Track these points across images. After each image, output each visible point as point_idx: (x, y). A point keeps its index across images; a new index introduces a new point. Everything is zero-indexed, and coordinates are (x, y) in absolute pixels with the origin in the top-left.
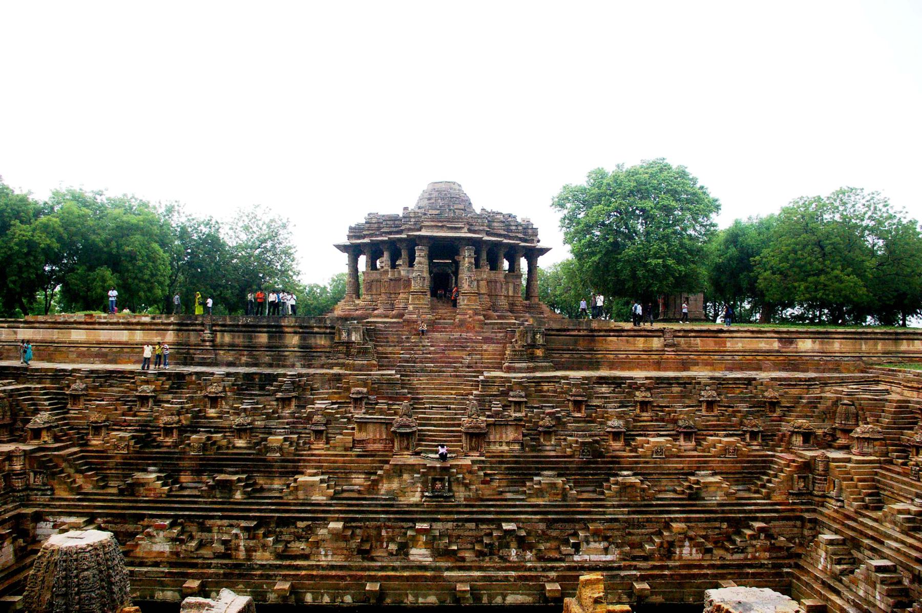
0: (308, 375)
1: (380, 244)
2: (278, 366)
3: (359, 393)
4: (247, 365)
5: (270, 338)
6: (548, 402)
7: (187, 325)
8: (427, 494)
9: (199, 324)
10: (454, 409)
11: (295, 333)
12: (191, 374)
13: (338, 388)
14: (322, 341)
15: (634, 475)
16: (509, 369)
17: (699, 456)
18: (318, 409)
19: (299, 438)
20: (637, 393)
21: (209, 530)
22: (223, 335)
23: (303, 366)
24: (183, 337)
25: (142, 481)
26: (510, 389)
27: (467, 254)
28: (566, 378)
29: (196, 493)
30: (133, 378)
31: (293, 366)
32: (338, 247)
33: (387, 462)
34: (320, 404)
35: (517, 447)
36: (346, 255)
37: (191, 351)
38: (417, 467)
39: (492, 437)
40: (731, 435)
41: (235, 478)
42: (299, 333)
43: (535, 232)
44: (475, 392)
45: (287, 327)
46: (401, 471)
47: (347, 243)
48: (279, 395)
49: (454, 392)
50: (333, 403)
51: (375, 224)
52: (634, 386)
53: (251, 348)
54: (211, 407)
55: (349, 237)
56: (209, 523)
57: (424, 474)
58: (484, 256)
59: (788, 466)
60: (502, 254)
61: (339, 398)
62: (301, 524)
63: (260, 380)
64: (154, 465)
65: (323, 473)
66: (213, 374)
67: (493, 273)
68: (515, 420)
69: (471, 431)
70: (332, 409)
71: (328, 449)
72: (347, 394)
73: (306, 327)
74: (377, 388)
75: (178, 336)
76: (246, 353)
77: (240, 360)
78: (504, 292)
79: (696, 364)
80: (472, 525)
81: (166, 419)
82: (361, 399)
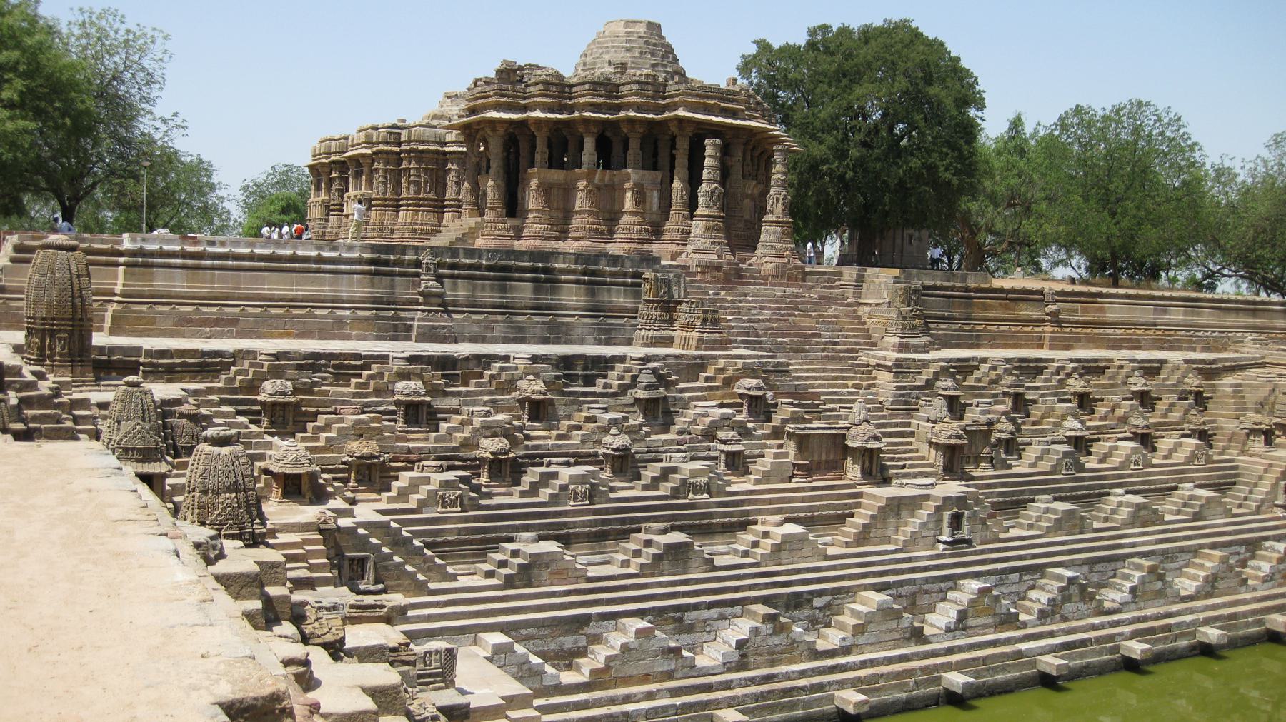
2: (557, 341)
4: (506, 340)
5: (536, 291)
6: (982, 396)
7: (387, 263)
9: (410, 264)
11: (577, 282)
12: (467, 359)
13: (707, 379)
20: (1071, 381)
21: (690, 629)
22: (454, 288)
23: (599, 342)
31: (582, 342)
37: (403, 314)
42: (584, 283)
45: (562, 271)
46: (899, 506)
56: (690, 616)
62: (818, 602)
64: (526, 528)
69: (953, 442)
72: (727, 390)
73: (593, 273)
76: (499, 318)
79: (1079, 340)
80: (1014, 577)
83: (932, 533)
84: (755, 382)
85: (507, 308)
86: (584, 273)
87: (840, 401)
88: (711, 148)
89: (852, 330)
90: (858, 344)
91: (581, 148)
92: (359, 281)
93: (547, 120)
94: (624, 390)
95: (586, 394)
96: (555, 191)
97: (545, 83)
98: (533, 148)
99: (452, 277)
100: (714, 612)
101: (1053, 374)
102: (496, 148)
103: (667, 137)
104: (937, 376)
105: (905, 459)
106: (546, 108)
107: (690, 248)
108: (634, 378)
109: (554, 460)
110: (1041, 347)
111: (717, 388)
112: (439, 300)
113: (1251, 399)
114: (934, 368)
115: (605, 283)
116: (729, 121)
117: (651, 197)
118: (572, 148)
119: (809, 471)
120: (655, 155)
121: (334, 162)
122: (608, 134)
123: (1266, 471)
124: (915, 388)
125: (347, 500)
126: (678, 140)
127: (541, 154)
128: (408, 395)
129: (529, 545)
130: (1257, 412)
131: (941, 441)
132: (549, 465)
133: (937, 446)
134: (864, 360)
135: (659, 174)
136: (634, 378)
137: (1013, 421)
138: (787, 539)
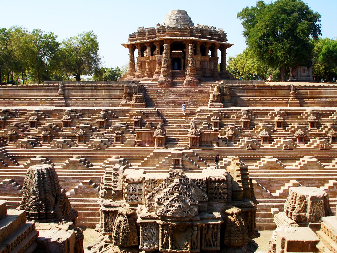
0: (111, 110)
1: (144, 43)
3: (138, 118)
4: (82, 106)
7: (51, 86)
10: (184, 126)
11: (105, 89)
15: (274, 157)
16: (211, 106)
17: (306, 149)
18: (118, 127)
19: (109, 141)
20: (276, 118)
26: (212, 115)
27: (190, 48)
28: (240, 110)
29: (60, 167)
30: (26, 113)
32: (123, 45)
33: (152, 152)
34: (118, 124)
36: (128, 49)
37: (54, 99)
39: (203, 139)
40: (322, 139)
41: (79, 160)
43: (225, 35)
44: (194, 118)
47: (129, 43)
48: (98, 120)
49: (184, 118)
50: (124, 124)
51: (142, 33)
52: (274, 115)
54: (65, 126)
55: (130, 40)
57: (169, 157)
58: (199, 48)
60: (208, 46)
61: (128, 121)
65: (121, 157)
66: (65, 110)
67: (203, 58)
68: (215, 131)
70: (124, 126)
71: (122, 146)
73: (110, 86)
74: (145, 116)
78: (209, 67)
81: (44, 132)
82: (138, 121)
86: (107, 86)
92: (43, 91)
94: (95, 119)
100: (75, 180)
104: (212, 115)
106: (140, 40)
109: (61, 137)
110: (287, 106)
115: (113, 89)
116: (184, 38)
119: (142, 144)
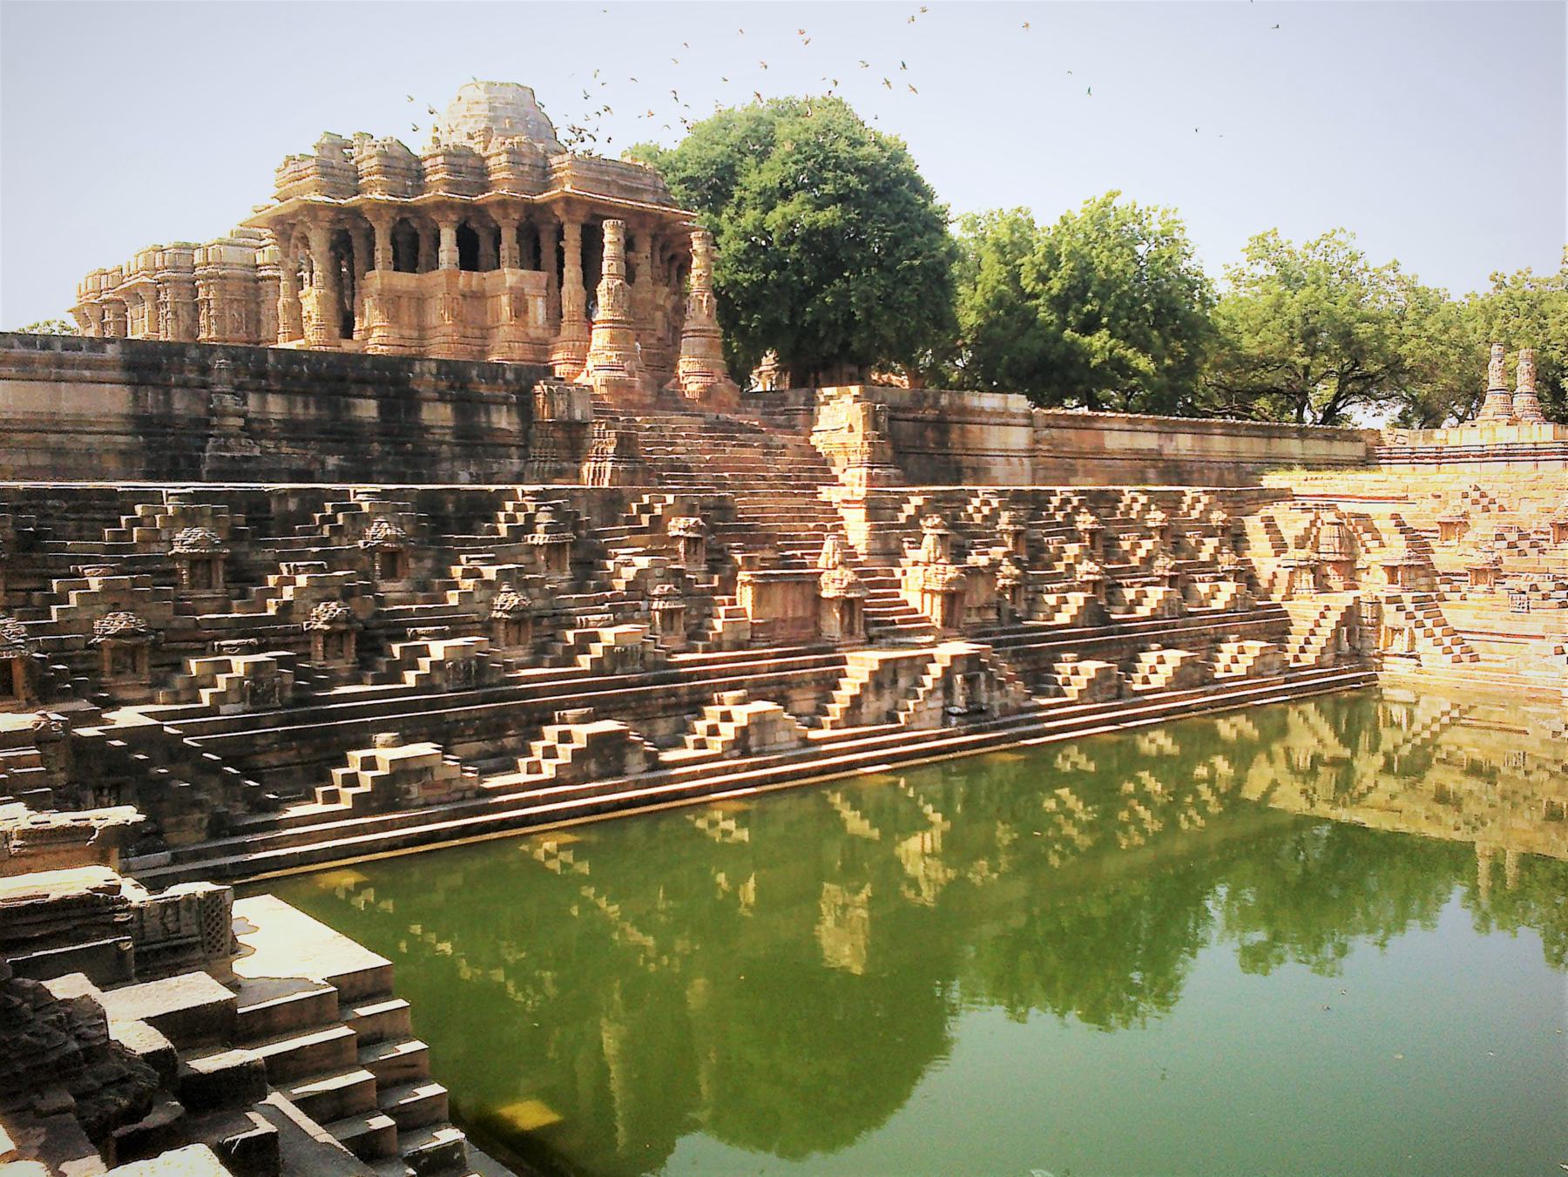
5: (381, 408)
8: (956, 710)
11: (442, 399)
12: (283, 496)
14: (503, 420)
22: (264, 402)
24: (150, 398)
25: (417, 766)
31: (453, 479)
35: (992, 615)
38: (918, 662)
46: (895, 673)
49: (811, 525)
53: (344, 435)
59: (1323, 616)
63: (458, 508)
75: (136, 399)
77: (323, 464)
83: (940, 703)
84: (692, 520)
85: (344, 435)
87: (801, 547)
88: (610, 235)
89: (805, 462)
90: (816, 479)
91: (438, 243)
92: (112, 393)
93: (389, 205)
94: (517, 533)
95: (464, 542)
96: (404, 301)
97: (384, 155)
98: (371, 245)
99: (257, 390)
101: (1058, 509)
102: (319, 241)
103: (551, 227)
104: (920, 512)
105: (894, 613)
107: (590, 365)
108: (530, 518)
109: (420, 630)
111: (642, 531)
112: (241, 422)
113: (1289, 534)
114: (917, 501)
117: (535, 307)
118: (424, 247)
120: (537, 251)
121: (106, 302)
122: (473, 225)
123: (1323, 616)
124: (901, 526)
125: (95, 701)
126: (566, 227)
127: (383, 249)
128: (192, 546)
129: (386, 753)
130: (1300, 545)
131: (939, 588)
132: (416, 636)
133: (932, 592)
134: (822, 498)
135: (542, 276)
136: (530, 518)
137: (1017, 563)
138: (760, 721)
